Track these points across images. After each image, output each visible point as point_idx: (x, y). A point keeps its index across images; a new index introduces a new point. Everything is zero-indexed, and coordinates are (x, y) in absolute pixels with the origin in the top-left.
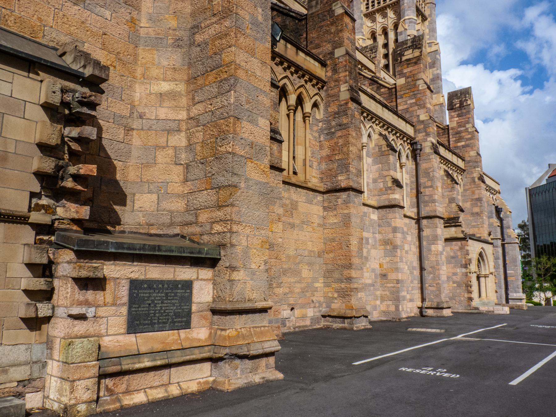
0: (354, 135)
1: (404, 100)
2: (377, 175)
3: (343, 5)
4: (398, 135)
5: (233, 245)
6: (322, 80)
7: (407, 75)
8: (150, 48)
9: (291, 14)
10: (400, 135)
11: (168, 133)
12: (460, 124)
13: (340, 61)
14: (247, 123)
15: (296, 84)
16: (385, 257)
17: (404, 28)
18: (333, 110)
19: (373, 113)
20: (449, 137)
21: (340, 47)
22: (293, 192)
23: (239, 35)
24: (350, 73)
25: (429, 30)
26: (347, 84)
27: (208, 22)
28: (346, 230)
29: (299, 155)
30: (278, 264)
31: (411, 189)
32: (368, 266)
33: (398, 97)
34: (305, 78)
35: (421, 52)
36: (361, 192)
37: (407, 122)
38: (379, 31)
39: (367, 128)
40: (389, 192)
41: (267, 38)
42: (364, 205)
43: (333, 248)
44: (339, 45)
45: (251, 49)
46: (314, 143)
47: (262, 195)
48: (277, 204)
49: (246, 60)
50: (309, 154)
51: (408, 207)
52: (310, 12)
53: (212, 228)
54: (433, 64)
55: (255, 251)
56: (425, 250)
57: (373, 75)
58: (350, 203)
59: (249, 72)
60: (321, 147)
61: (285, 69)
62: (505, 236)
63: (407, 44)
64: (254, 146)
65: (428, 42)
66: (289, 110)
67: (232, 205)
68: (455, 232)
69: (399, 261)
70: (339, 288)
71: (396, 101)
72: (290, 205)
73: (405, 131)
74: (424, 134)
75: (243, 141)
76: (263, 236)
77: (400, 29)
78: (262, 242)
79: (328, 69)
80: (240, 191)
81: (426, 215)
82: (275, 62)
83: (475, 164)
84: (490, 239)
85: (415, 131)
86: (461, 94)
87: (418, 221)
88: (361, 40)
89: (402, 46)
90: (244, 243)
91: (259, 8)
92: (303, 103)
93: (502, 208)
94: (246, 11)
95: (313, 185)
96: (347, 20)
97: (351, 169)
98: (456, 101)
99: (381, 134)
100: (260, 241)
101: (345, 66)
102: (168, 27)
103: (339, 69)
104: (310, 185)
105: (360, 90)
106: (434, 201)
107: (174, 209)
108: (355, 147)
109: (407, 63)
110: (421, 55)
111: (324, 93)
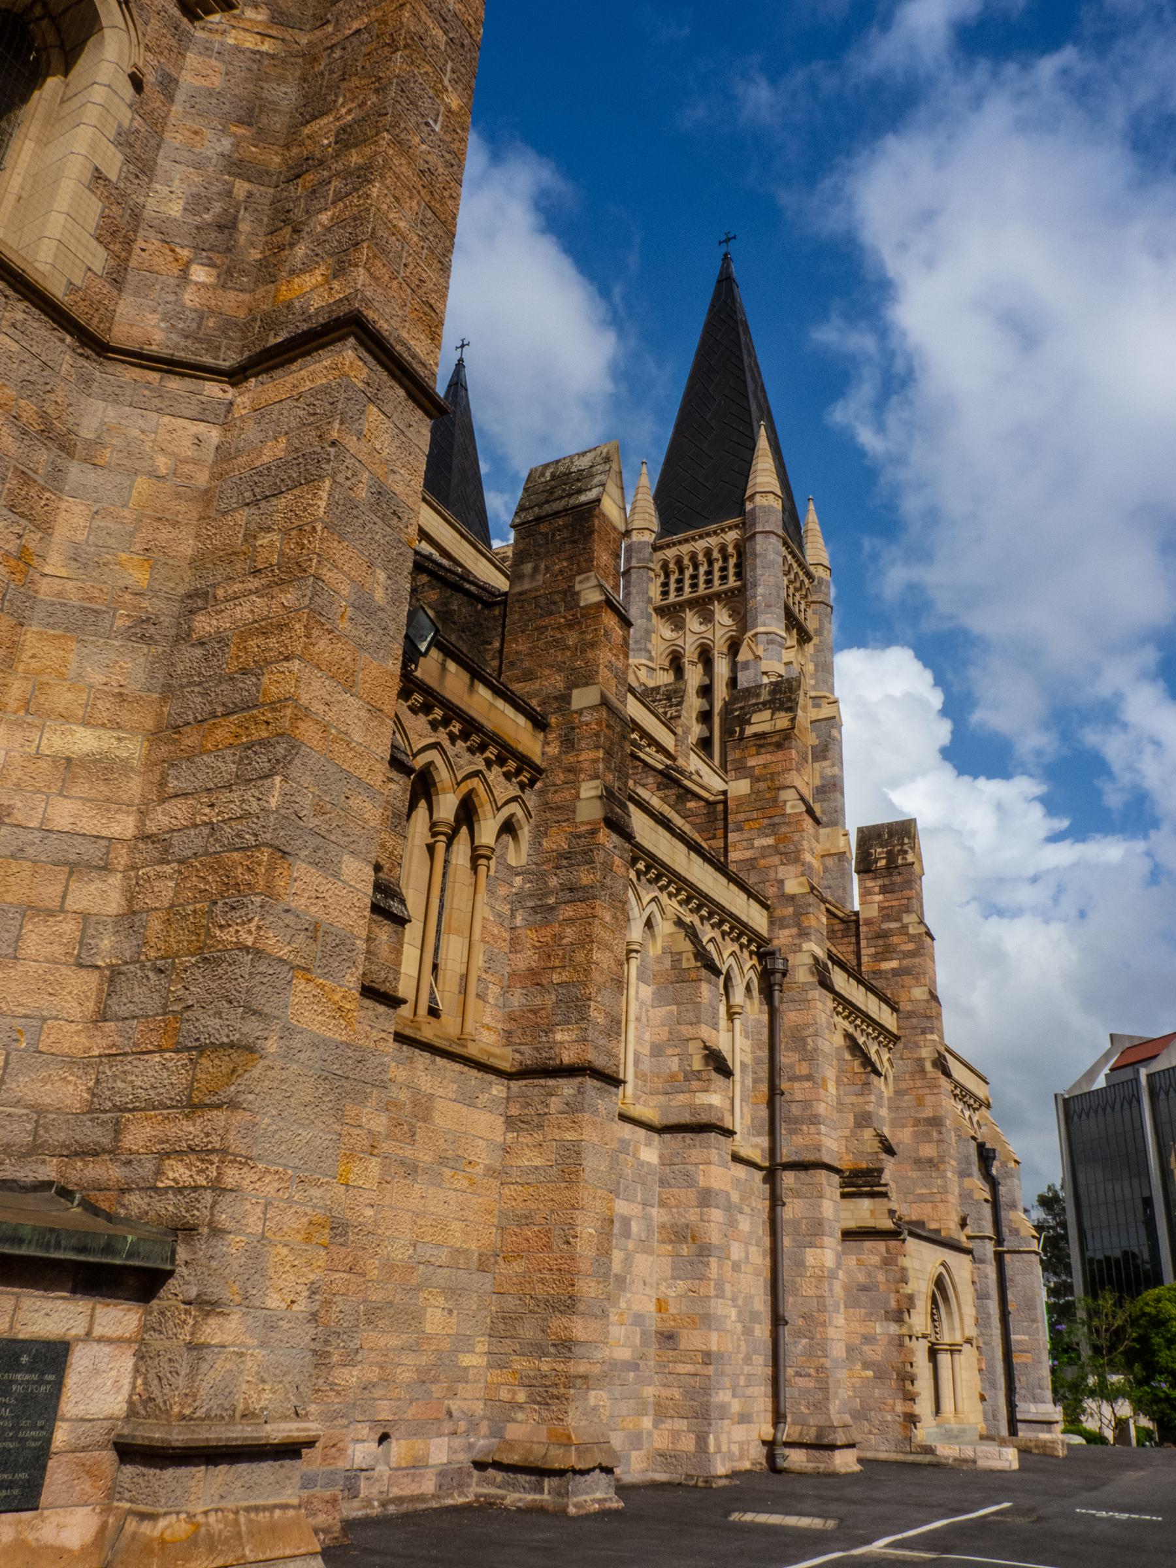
0: (608, 919)
1: (746, 835)
2: (664, 1036)
3: (603, 582)
4: (726, 927)
5: (217, 1232)
6: (533, 762)
7: (757, 772)
8: (58, 632)
9: (467, 586)
10: (732, 928)
11: (71, 873)
12: (888, 911)
13: (583, 719)
14: (309, 868)
15: (461, 768)
16: (673, 1278)
17: (754, 653)
18: (555, 847)
19: (663, 865)
20: (858, 943)
21: (587, 684)
22: (421, 1067)
23: (315, 632)
24: (609, 753)
25: (816, 665)
26: (597, 782)
27: (237, 587)
28: (567, 1193)
29: (449, 962)
30: (352, 1288)
31: (755, 1081)
32: (623, 1305)
33: (731, 826)
34: (487, 754)
35: (793, 720)
36: (615, 1081)
37: (750, 895)
38: (690, 652)
39: (645, 903)
40: (695, 1084)
41: (392, 649)
42: (624, 1118)
43: (525, 1245)
44: (587, 679)
45: (346, 672)
46: (496, 932)
47: (326, 1078)
48: (372, 1103)
49: (328, 697)
50: (479, 960)
51: (745, 1131)
52: (517, 589)
53: (159, 1173)
54: (823, 751)
55: (285, 1251)
56: (786, 1262)
57: (669, 762)
58: (582, 1110)
59: (333, 731)
60: (515, 944)
61: (434, 725)
62: (1005, 1231)
63: (758, 695)
64: (320, 934)
65: (813, 694)
66: (434, 835)
67: (233, 1105)
68: (872, 1212)
69: (713, 1293)
70: (532, 1373)
71: (726, 837)
72: (408, 1108)
73: (744, 918)
74: (794, 931)
75: (289, 919)
76: (314, 1207)
77: (744, 655)
78: (311, 1223)
79: (551, 737)
80: (262, 1064)
81: (794, 1158)
82: (409, 703)
83: (926, 1023)
84: (964, 1239)
85: (771, 923)
86: (891, 835)
87: (771, 1174)
88: (644, 669)
89: (746, 699)
90: (254, 1225)
91: (378, 571)
92: (475, 818)
93: (994, 1150)
94: (344, 573)
95: (483, 1050)
96: (609, 620)
97: (593, 1013)
98: (879, 851)
99: (679, 923)
100: (305, 1220)
101: (597, 735)
102: (121, 583)
103: (579, 740)
104: (472, 1050)
105: (631, 799)
106: (815, 1120)
107: (48, 1101)
108: (608, 954)
109: (758, 742)
110: (793, 728)
111: (533, 797)
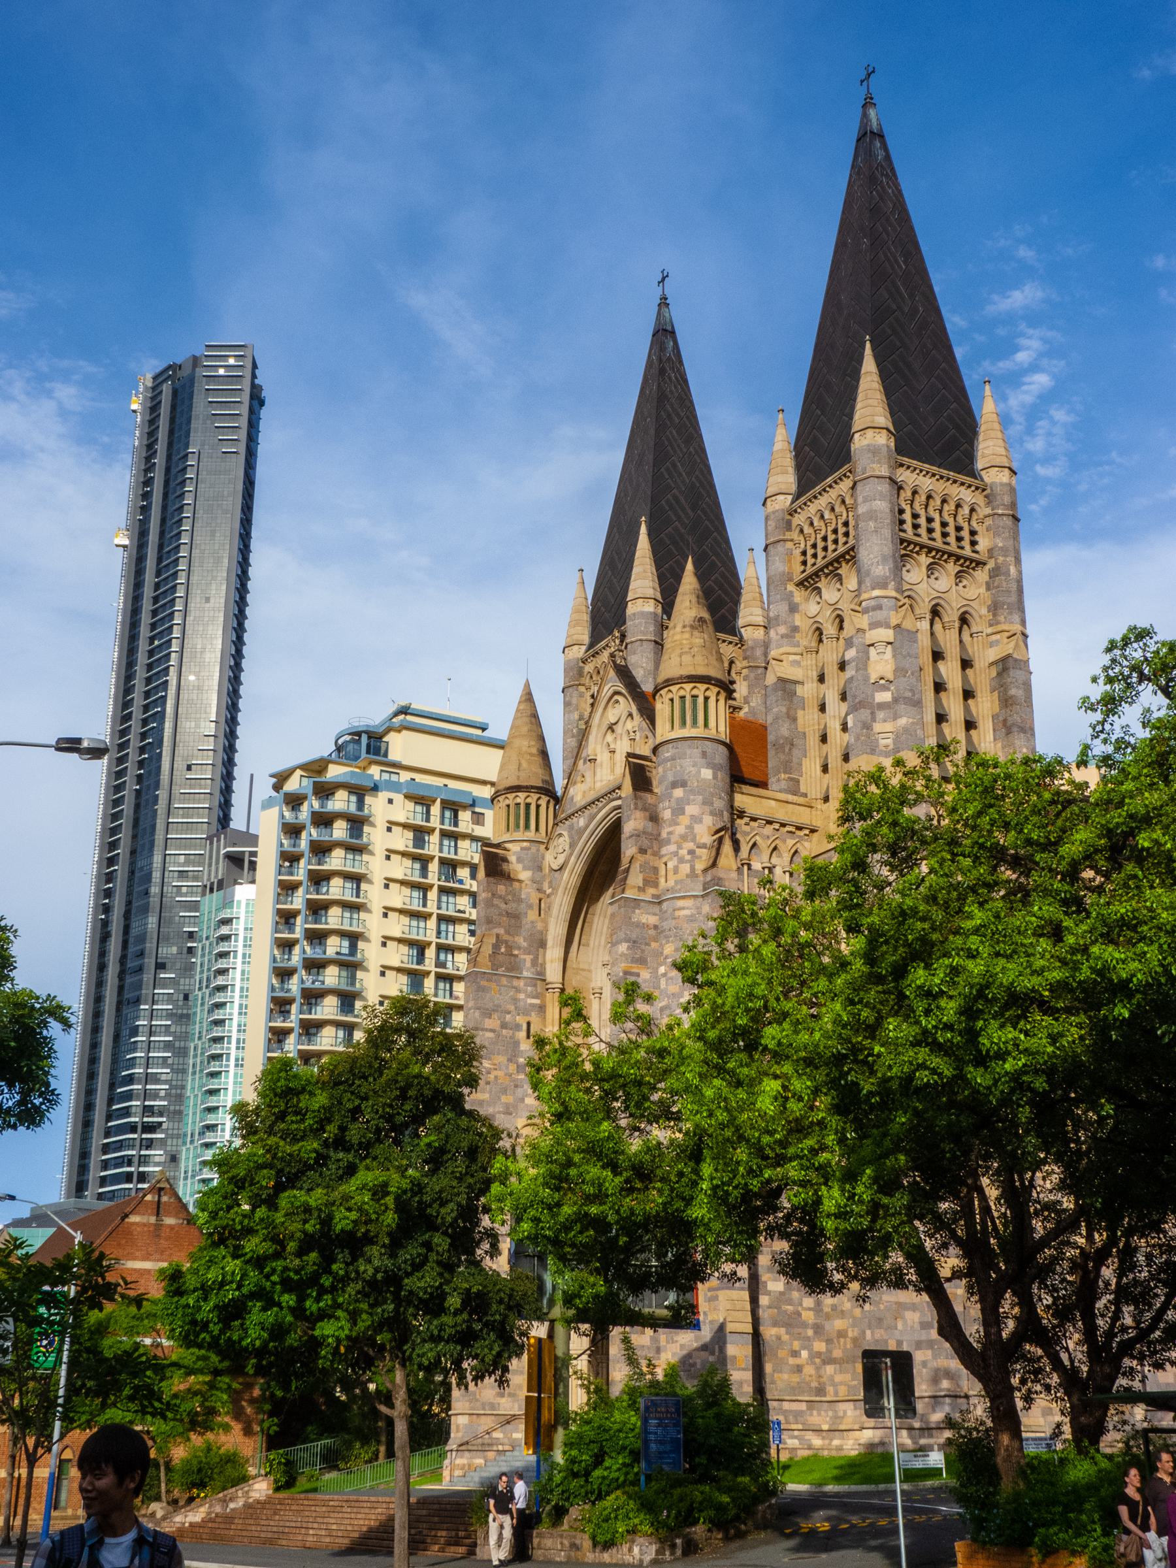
77: (848, 630)
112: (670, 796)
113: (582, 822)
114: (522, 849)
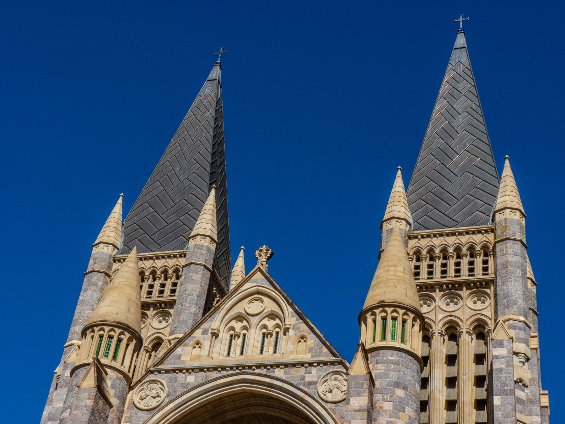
17: (507, 334)
112: (392, 394)
113: (191, 379)
114: (118, 378)
